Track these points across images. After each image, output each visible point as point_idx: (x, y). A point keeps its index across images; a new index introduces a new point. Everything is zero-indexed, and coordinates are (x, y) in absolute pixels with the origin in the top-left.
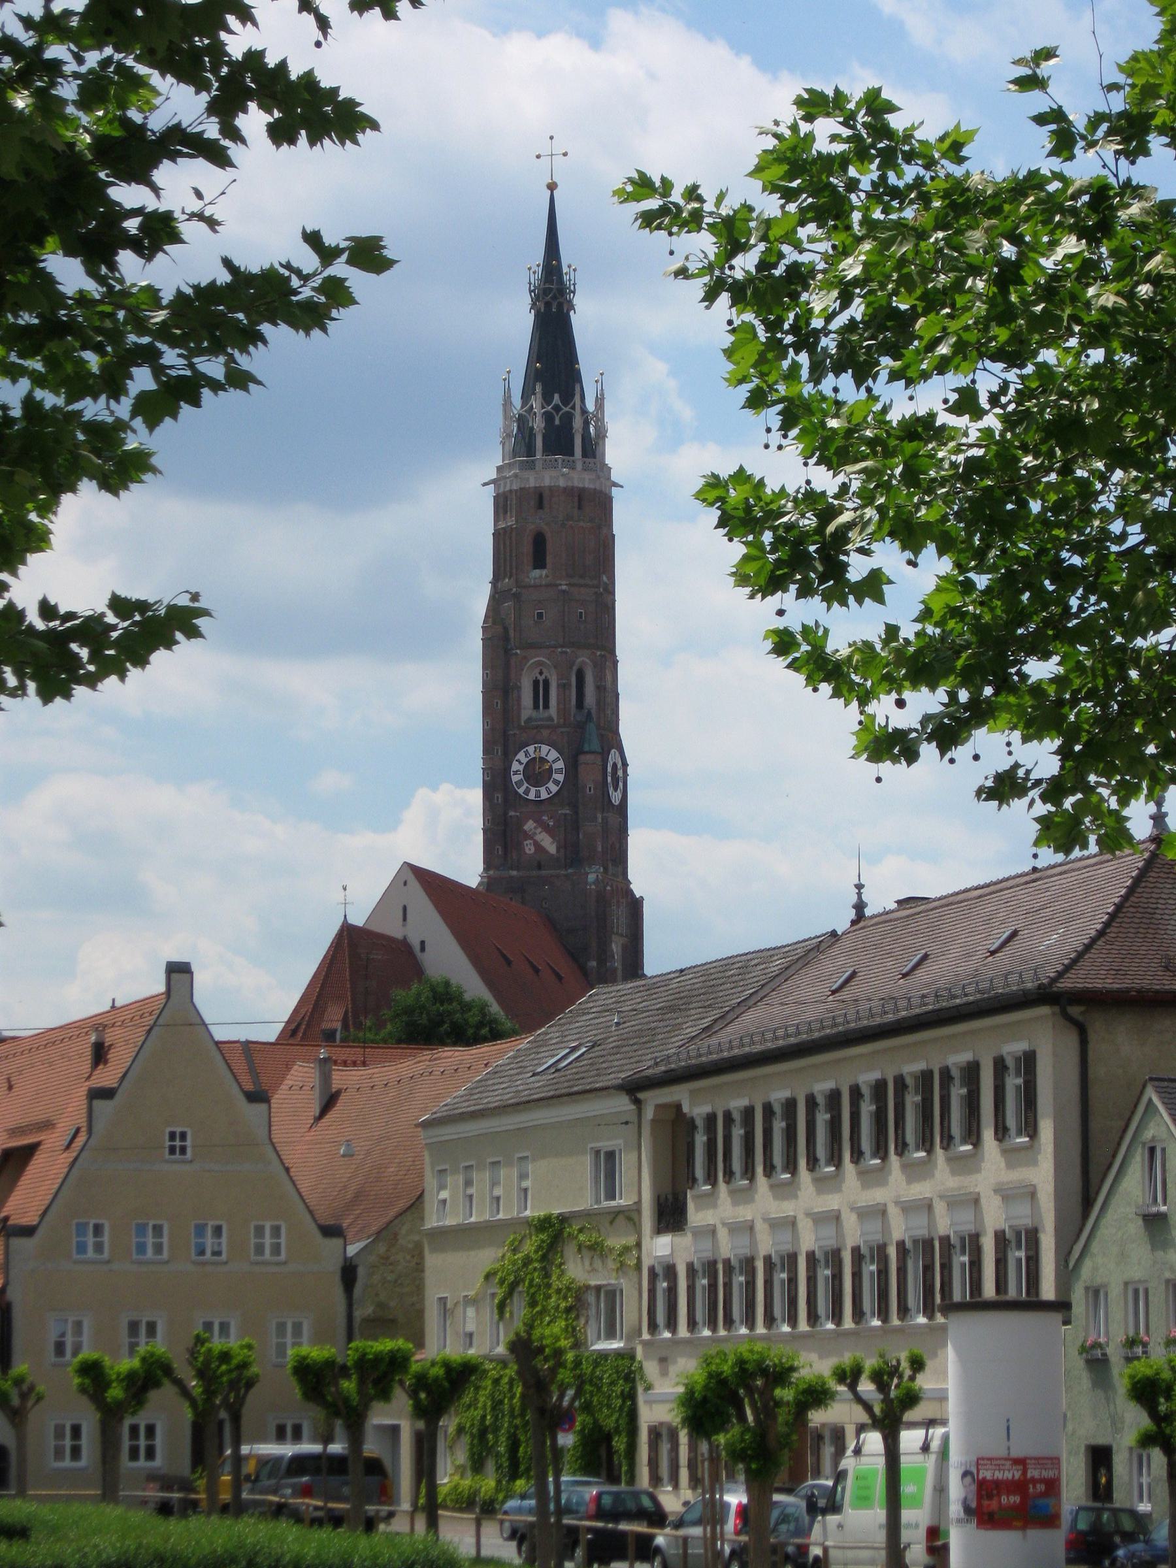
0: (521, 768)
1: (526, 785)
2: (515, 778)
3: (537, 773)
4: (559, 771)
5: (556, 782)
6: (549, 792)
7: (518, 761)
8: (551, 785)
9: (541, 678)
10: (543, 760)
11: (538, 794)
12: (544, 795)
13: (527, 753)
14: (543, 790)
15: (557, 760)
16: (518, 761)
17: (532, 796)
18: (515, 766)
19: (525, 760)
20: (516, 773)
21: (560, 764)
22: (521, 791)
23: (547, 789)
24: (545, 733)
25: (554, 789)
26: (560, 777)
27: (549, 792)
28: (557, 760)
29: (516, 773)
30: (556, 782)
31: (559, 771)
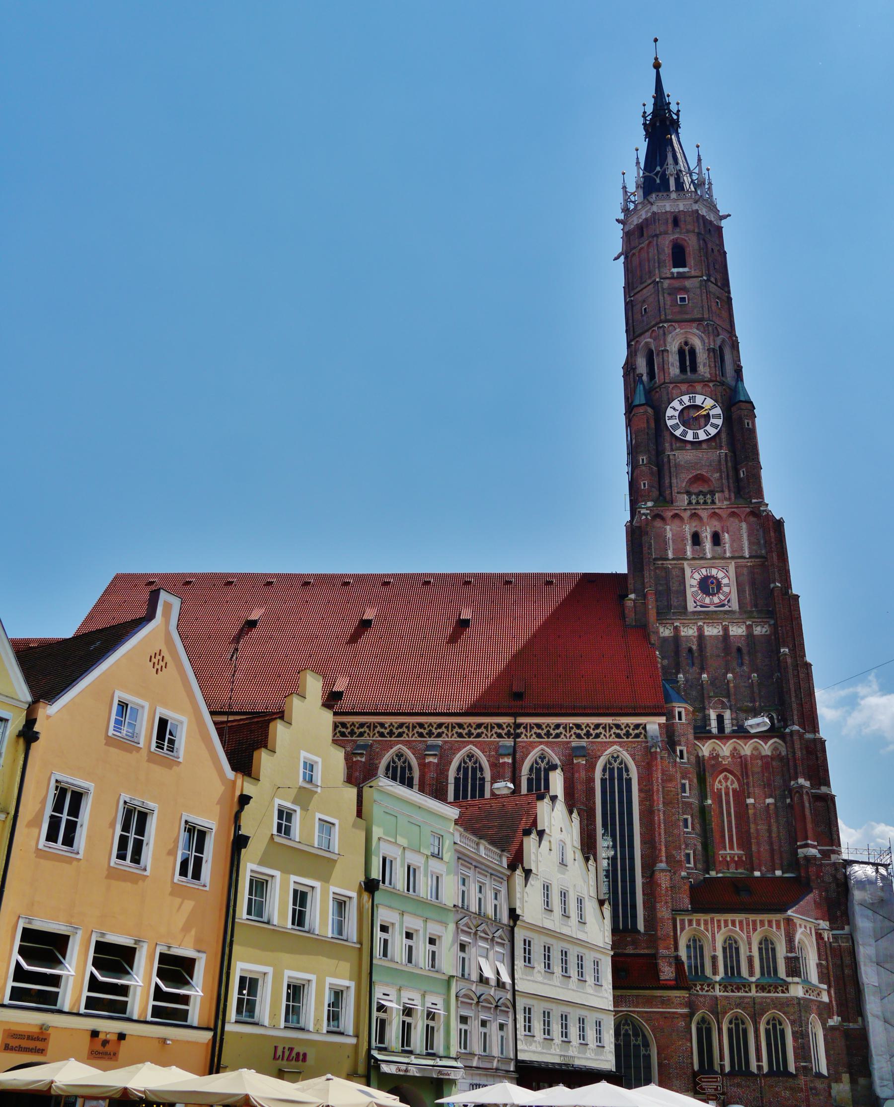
0: (677, 414)
1: (682, 428)
2: (670, 423)
3: (692, 417)
4: (717, 416)
5: (715, 426)
6: (707, 433)
7: (674, 409)
8: (708, 428)
9: (687, 348)
10: (699, 408)
11: (696, 436)
12: (702, 436)
13: (681, 402)
15: (713, 407)
16: (674, 409)
17: (690, 437)
18: (670, 412)
19: (680, 408)
20: (671, 418)
21: (718, 411)
22: (678, 433)
24: (699, 387)
25: (713, 432)
26: (719, 422)
28: (713, 407)
29: (671, 418)
30: (715, 426)
31: (717, 416)
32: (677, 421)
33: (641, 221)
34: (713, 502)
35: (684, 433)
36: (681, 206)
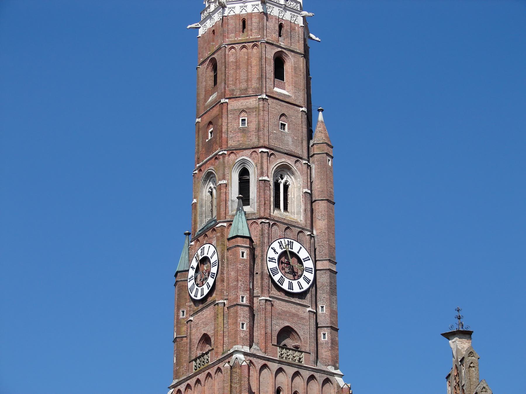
6: (301, 287)
7: (275, 251)
8: (301, 280)
11: (291, 286)
12: (296, 289)
14: (295, 283)
16: (275, 251)
18: (271, 254)
19: (280, 251)
20: (272, 260)
21: (309, 264)
22: (276, 278)
23: (299, 283)
25: (306, 286)
26: (311, 277)
27: (301, 287)
29: (272, 260)
30: (307, 280)
31: (308, 270)
32: (276, 265)
33: (244, 12)
34: (299, 361)
35: (281, 281)
36: (288, 16)
